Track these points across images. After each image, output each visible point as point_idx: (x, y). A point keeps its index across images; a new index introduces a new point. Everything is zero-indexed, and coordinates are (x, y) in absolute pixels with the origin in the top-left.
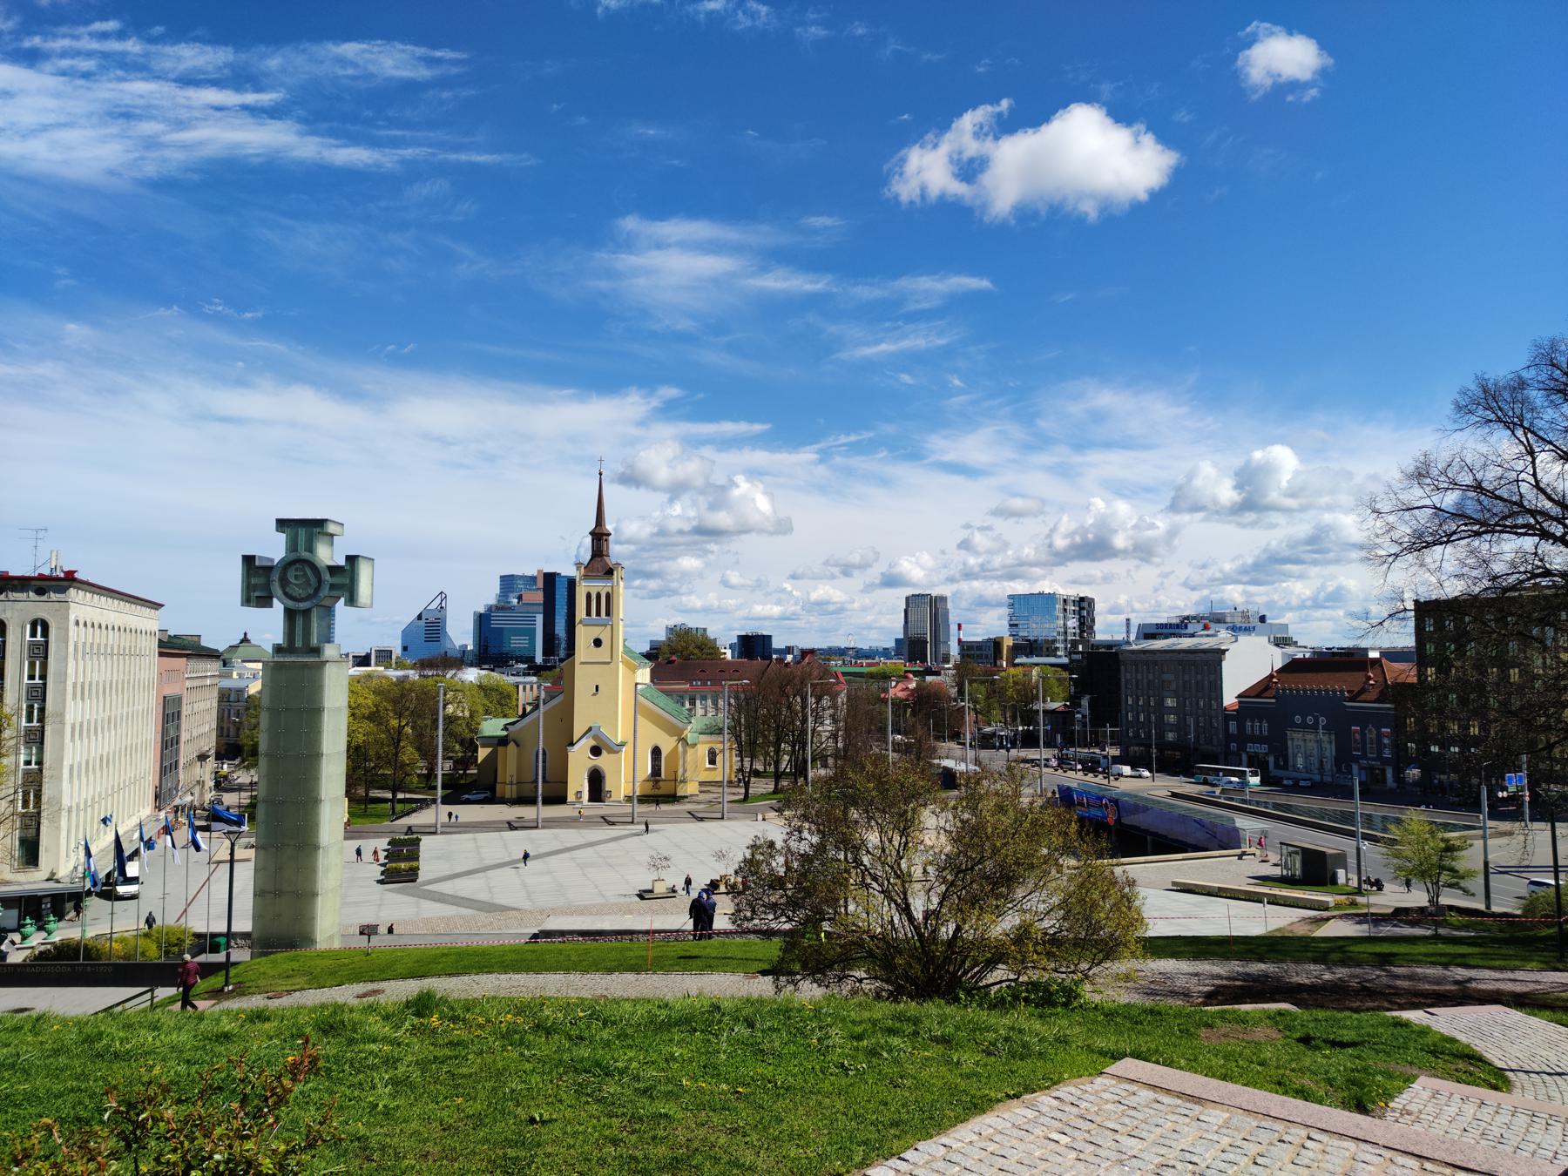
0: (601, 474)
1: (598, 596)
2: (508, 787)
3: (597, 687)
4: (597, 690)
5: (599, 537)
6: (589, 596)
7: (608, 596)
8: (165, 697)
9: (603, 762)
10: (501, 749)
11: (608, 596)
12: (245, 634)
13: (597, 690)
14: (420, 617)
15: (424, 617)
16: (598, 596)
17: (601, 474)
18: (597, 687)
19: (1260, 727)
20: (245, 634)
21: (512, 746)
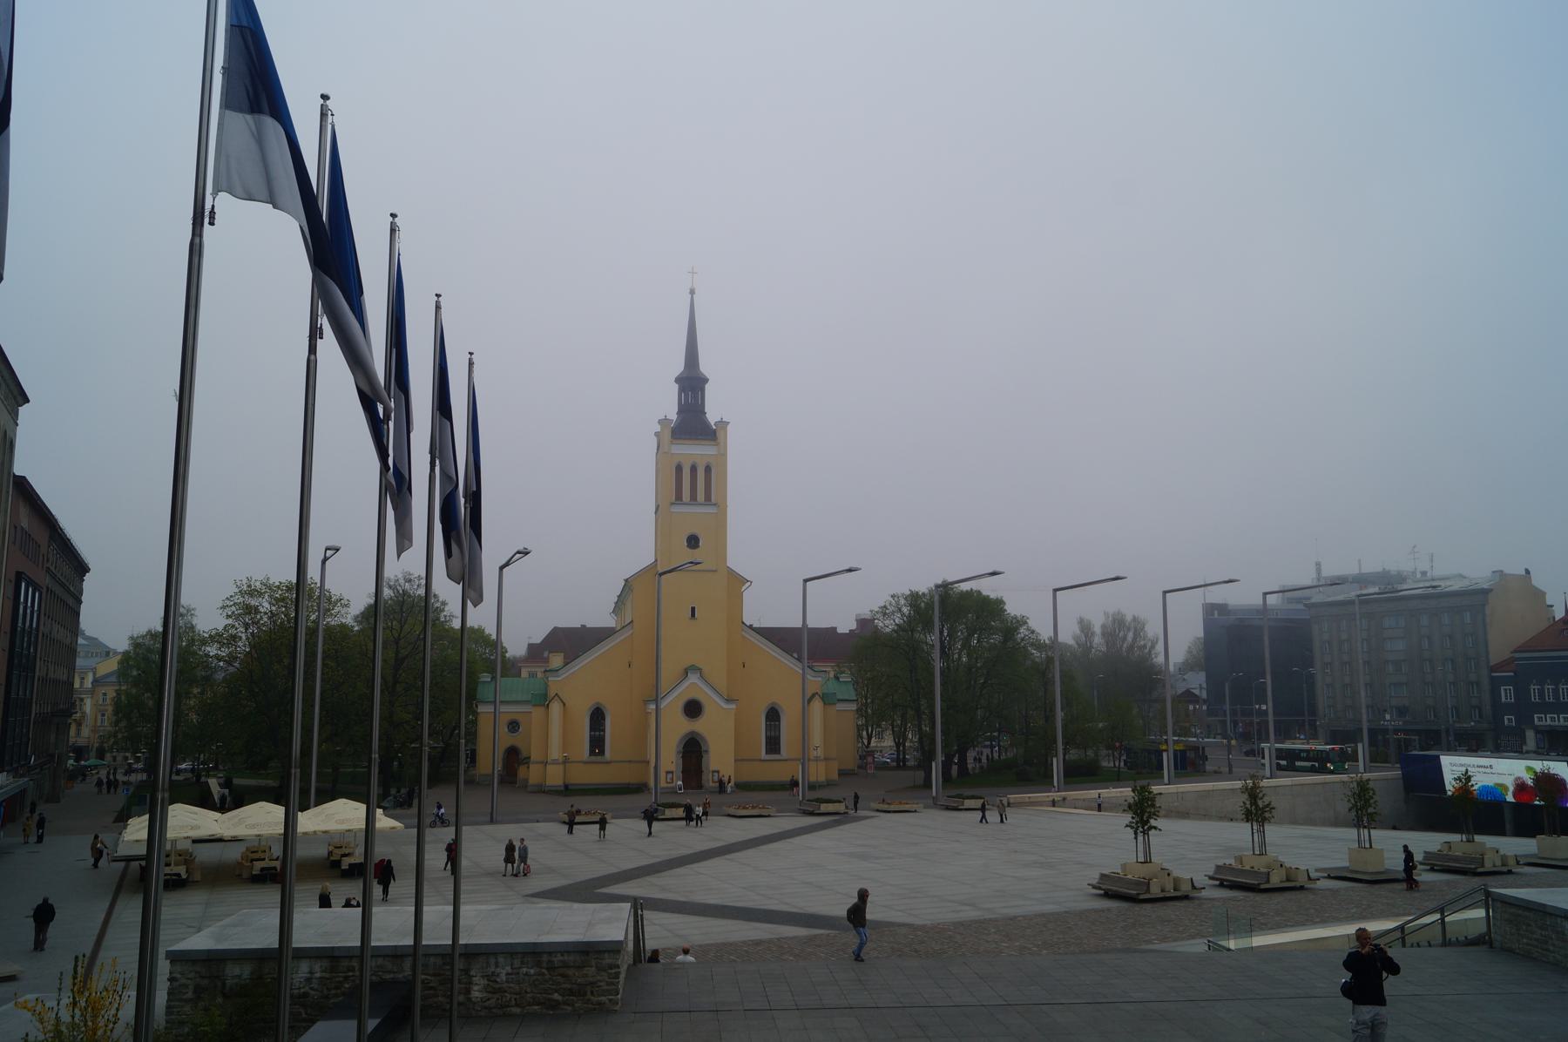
0: (692, 292)
1: (694, 469)
3: (693, 609)
4: (693, 614)
6: (679, 469)
9: (700, 726)
11: (708, 469)
13: (693, 614)
16: (694, 469)
17: (692, 292)
18: (693, 609)
19: (1556, 691)
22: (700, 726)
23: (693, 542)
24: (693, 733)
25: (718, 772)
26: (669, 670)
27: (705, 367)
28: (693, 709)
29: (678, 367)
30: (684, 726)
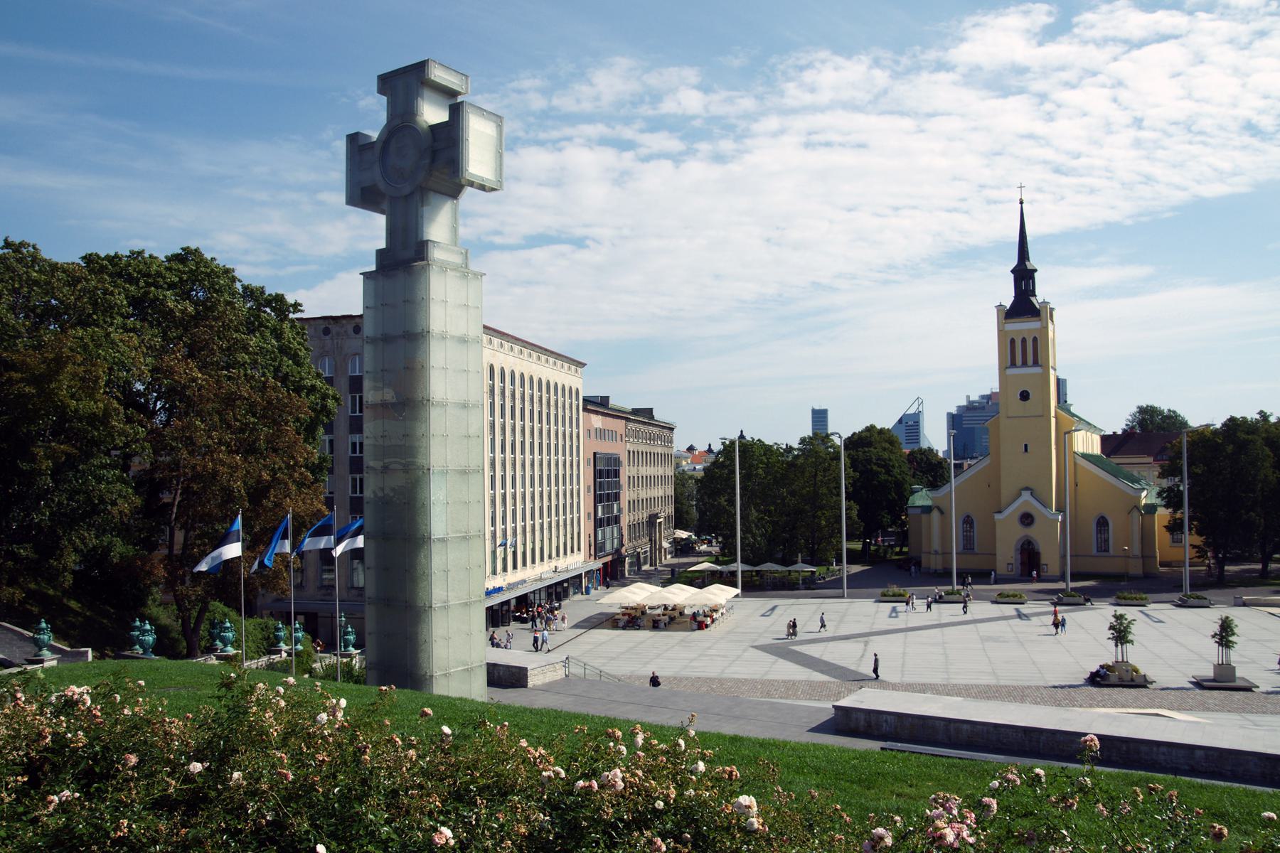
0: (1021, 203)
1: (1024, 340)
2: (933, 557)
3: (1026, 446)
5: (1024, 276)
6: (1013, 342)
7: (1035, 340)
8: (595, 454)
10: (924, 517)
11: (1035, 340)
12: (742, 432)
14: (900, 421)
15: (904, 422)
16: (1024, 340)
17: (1021, 203)
18: (1026, 446)
20: (742, 432)
21: (935, 514)
22: (1033, 532)
23: (1025, 396)
24: (1026, 536)
25: (1046, 565)
26: (1006, 492)
27: (1033, 262)
28: (1027, 519)
29: (1014, 263)
30: (1019, 532)
